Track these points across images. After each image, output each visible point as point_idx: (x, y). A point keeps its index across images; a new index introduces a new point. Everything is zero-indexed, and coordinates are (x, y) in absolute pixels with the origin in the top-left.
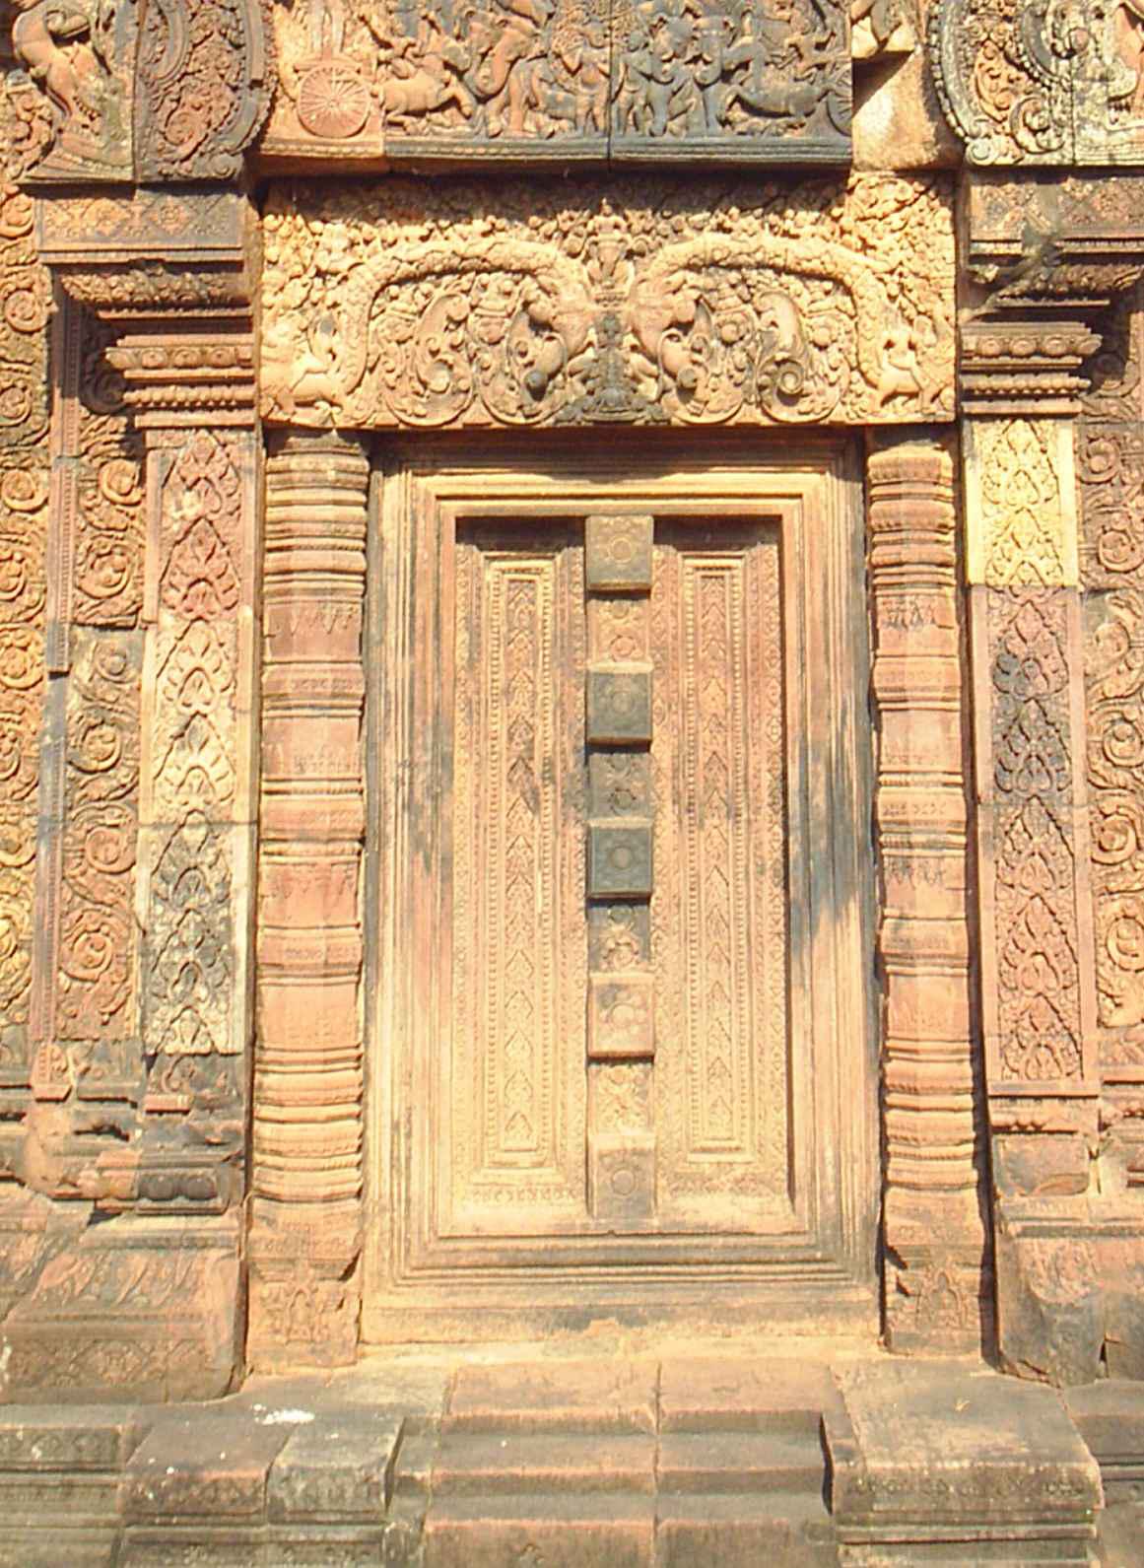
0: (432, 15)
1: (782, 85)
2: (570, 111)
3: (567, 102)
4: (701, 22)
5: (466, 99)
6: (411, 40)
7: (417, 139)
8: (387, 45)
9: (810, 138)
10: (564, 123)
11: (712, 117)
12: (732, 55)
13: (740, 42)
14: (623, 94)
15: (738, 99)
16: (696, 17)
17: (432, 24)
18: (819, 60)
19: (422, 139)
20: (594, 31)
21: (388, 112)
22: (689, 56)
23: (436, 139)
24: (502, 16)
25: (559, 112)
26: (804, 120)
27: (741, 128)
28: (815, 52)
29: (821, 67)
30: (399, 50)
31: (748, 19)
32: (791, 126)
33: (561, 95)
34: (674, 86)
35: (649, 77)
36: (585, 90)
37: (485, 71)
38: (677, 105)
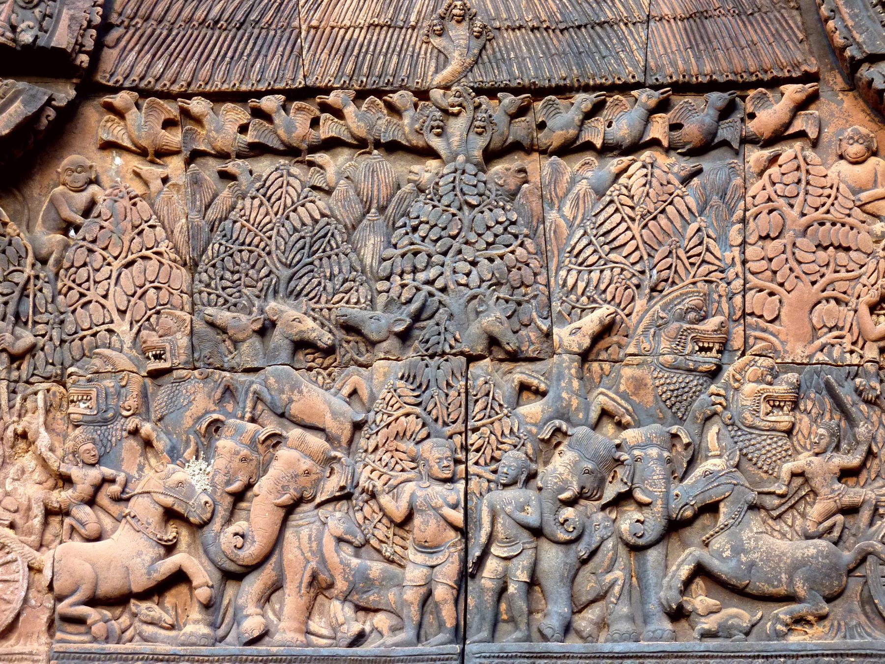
0: (147, 428)
1: (781, 545)
2: (392, 595)
3: (389, 581)
4: (630, 435)
5: (201, 573)
6: (107, 471)
7: (112, 647)
8: (66, 480)
9: (836, 641)
10: (381, 620)
11: (653, 606)
12: (689, 491)
13: (698, 471)
14: (492, 566)
15: (700, 571)
16: (621, 426)
17: (148, 444)
18: (847, 500)
19: (120, 648)
20: (435, 452)
21: (60, 599)
22: (610, 492)
23: (147, 647)
24: (271, 427)
25: (372, 598)
26: (826, 608)
27: (709, 623)
28: (837, 486)
29: (850, 511)
30: (83, 488)
31: (713, 431)
32: (800, 620)
33: (376, 568)
34: (582, 550)
35: (537, 532)
36: (420, 558)
37: (239, 525)
38: (587, 585)
